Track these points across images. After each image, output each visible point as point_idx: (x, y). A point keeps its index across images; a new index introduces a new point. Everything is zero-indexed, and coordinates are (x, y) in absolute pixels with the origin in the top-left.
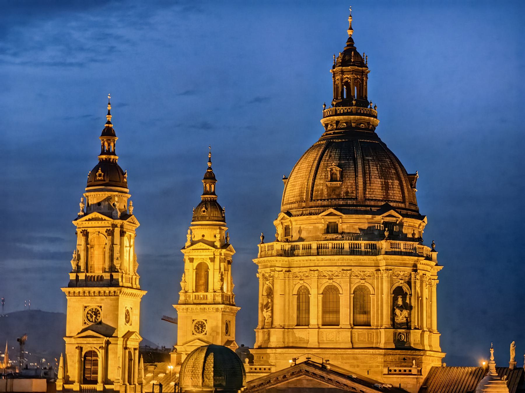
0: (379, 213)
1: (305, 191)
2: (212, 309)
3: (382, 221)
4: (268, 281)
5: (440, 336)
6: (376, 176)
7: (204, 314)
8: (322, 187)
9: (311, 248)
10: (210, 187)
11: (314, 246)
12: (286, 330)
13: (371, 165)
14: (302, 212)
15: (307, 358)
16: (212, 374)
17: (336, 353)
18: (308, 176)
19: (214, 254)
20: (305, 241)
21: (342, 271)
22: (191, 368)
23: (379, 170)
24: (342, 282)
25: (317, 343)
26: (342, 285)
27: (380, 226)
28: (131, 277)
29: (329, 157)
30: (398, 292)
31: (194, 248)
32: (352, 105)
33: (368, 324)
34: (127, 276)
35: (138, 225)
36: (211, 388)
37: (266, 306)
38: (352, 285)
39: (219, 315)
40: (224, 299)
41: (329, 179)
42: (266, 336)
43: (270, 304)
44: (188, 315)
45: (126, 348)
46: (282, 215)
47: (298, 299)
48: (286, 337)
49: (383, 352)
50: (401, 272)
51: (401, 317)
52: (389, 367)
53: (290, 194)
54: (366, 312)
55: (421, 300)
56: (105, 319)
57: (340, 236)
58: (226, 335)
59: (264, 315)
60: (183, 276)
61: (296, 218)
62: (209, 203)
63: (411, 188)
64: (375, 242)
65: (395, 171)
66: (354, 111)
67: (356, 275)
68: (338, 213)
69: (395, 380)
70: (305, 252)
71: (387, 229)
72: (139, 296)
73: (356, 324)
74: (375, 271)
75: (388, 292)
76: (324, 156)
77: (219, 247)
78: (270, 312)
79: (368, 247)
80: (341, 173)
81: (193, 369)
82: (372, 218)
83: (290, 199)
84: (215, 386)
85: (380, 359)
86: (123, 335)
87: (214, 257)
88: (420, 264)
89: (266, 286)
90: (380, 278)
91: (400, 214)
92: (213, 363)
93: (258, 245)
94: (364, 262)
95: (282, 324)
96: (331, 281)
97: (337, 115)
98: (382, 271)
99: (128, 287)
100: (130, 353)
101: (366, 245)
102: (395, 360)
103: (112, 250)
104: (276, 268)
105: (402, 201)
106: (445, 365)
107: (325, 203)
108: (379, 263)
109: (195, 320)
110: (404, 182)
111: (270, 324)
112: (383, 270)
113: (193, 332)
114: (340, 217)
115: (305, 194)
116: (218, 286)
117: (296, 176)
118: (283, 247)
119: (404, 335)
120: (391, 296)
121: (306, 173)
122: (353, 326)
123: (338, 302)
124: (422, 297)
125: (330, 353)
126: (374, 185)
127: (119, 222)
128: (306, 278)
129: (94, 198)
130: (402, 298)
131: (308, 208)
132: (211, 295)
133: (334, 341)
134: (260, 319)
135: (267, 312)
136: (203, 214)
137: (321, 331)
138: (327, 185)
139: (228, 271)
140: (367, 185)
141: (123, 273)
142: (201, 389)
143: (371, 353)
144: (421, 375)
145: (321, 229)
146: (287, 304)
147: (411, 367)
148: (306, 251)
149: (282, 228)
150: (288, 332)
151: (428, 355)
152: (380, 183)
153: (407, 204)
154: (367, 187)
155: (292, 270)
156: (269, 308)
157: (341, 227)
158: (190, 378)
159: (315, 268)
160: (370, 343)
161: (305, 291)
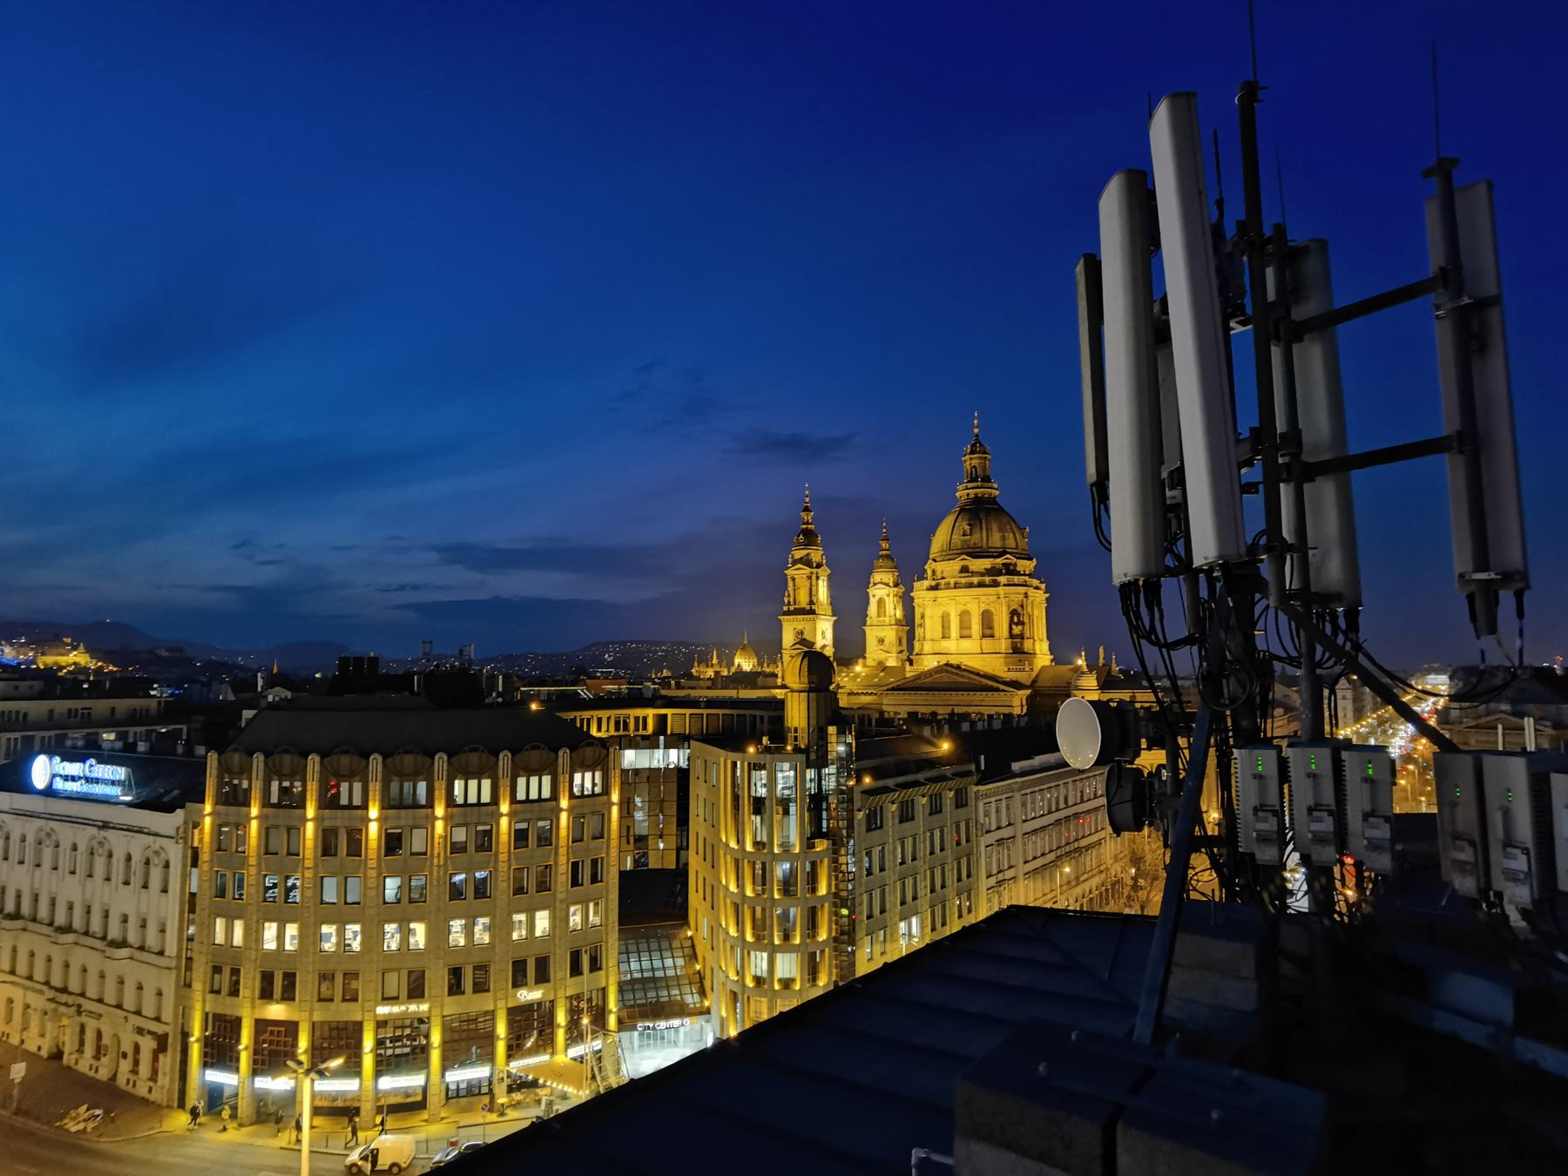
30: (1014, 613)
35: (829, 572)
37: (921, 625)
39: (894, 633)
46: (930, 561)
54: (992, 628)
56: (807, 636)
59: (919, 632)
73: (984, 636)
80: (971, 530)
84: (809, 683)
85: (1002, 661)
97: (967, 489)
103: (811, 590)
107: (959, 551)
116: (892, 613)
123: (970, 620)
127: (815, 570)
129: (799, 554)
134: (917, 634)
157: (972, 568)
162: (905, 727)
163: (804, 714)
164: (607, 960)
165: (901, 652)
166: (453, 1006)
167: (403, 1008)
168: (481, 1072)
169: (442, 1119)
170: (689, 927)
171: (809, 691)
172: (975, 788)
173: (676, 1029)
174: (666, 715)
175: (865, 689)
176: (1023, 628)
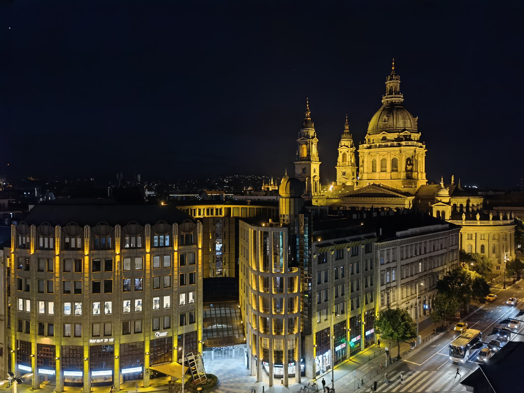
0: (402, 131)
11: (378, 145)
32: (393, 94)
33: (397, 171)
35: (318, 141)
37: (362, 166)
39: (350, 169)
45: (314, 181)
46: (367, 135)
47: (373, 163)
54: (397, 167)
59: (361, 169)
66: (394, 97)
68: (386, 133)
69: (406, 190)
73: (392, 171)
80: (388, 119)
84: (290, 194)
85: (401, 182)
91: (410, 132)
97: (387, 98)
100: (316, 182)
106: (428, 184)
107: (382, 130)
116: (350, 160)
123: (386, 164)
124: (418, 161)
134: (360, 170)
153: (413, 128)
157: (388, 138)
162: (343, 215)
163: (288, 208)
164: (198, 318)
165: (353, 179)
166: (124, 340)
167: (102, 340)
168: (139, 369)
169: (121, 390)
170: (239, 304)
171: (290, 198)
172: (376, 244)
173: (231, 350)
174: (230, 208)
176: (412, 167)
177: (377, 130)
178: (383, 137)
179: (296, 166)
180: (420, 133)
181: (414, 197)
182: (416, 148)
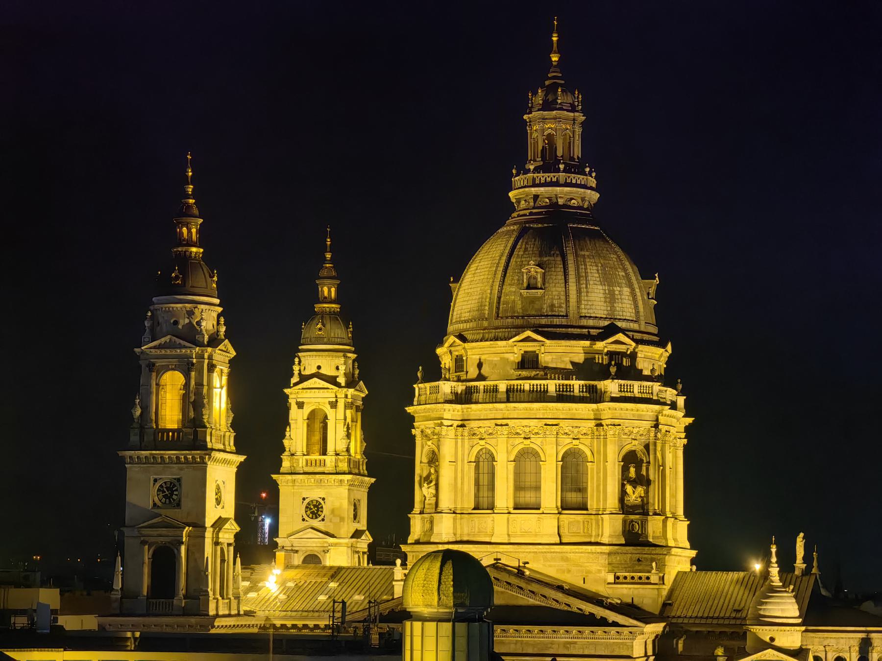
0: (602, 337)
1: (487, 304)
2: (333, 482)
3: (606, 350)
4: (431, 441)
5: (688, 525)
6: (596, 280)
7: (320, 490)
8: (513, 297)
9: (497, 391)
10: (330, 291)
11: (502, 386)
12: (458, 515)
13: (588, 264)
14: (483, 336)
15: (495, 559)
16: (452, 589)
17: (536, 550)
18: (491, 280)
19: (336, 397)
20: (487, 380)
21: (545, 426)
22: (422, 582)
23: (600, 271)
24: (545, 444)
25: (506, 536)
26: (544, 447)
27: (602, 358)
28: (222, 434)
29: (524, 252)
30: (630, 459)
31: (305, 387)
34: (218, 432)
35: (233, 353)
36: (450, 608)
37: (428, 479)
38: (560, 448)
39: (344, 491)
40: (352, 466)
41: (525, 285)
42: (428, 526)
43: (433, 477)
44: (295, 490)
45: (217, 543)
46: (451, 339)
47: (477, 468)
48: (458, 527)
49: (607, 549)
50: (635, 429)
51: (633, 498)
52: (615, 573)
53: (464, 307)
54: (582, 490)
55: (662, 470)
57: (542, 373)
58: (354, 522)
59: (422, 493)
60: (288, 429)
61: (474, 344)
62: (328, 317)
63: (649, 299)
64: (595, 382)
65: (624, 274)
66: (562, 181)
67: (566, 433)
68: (539, 338)
69: (625, 592)
70: (488, 397)
71: (613, 363)
72: (234, 463)
73: (565, 506)
74: (595, 426)
75: (615, 459)
76: (515, 250)
77: (343, 384)
78: (434, 487)
79: (584, 390)
81: (425, 582)
82: (591, 346)
83: (463, 315)
84: (455, 605)
85: (603, 560)
86: (212, 523)
87: (337, 401)
88: (662, 415)
89: (426, 449)
90: (602, 437)
91: (633, 339)
92: (452, 574)
93: (415, 386)
94: (578, 413)
95: (452, 506)
96: (527, 442)
97: (534, 185)
98: (605, 427)
99: (219, 450)
100: (222, 550)
101: (581, 387)
102: (626, 561)
104: (443, 421)
105: (635, 319)
106: (694, 568)
107: (519, 322)
108: (600, 415)
109: (307, 498)
110: (637, 290)
111: (434, 507)
112: (607, 425)
113: (303, 517)
114: (541, 343)
115: (487, 308)
117: (472, 279)
118: (453, 389)
119: (638, 524)
120: (619, 465)
121: (488, 274)
122: (560, 510)
123: (538, 473)
124: (664, 465)
125: (526, 550)
126: (593, 294)
128: (489, 437)
130: (634, 467)
131: (492, 329)
132: (331, 459)
133: (531, 532)
135: (428, 488)
136: (319, 334)
137: (512, 518)
138: (521, 293)
139: (357, 422)
140: (583, 294)
141: (213, 429)
142: (436, 610)
143: (590, 551)
144: (664, 584)
145: (513, 362)
146: (459, 475)
147: (649, 572)
148: (490, 395)
149: (451, 360)
150: (461, 519)
151: (673, 553)
152: (602, 291)
153: (643, 323)
154: (583, 298)
155: (468, 424)
156: (431, 482)
157: (546, 359)
158: (421, 594)
159: (504, 422)
160: (586, 536)
161: (488, 456)
165: (357, 534)
171: (456, 619)
175: (313, 618)
176: (647, 492)
177: (498, 323)
178: (523, 356)
179: (133, 472)
180: (669, 347)
181: (658, 628)
182: (660, 412)
